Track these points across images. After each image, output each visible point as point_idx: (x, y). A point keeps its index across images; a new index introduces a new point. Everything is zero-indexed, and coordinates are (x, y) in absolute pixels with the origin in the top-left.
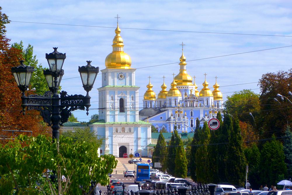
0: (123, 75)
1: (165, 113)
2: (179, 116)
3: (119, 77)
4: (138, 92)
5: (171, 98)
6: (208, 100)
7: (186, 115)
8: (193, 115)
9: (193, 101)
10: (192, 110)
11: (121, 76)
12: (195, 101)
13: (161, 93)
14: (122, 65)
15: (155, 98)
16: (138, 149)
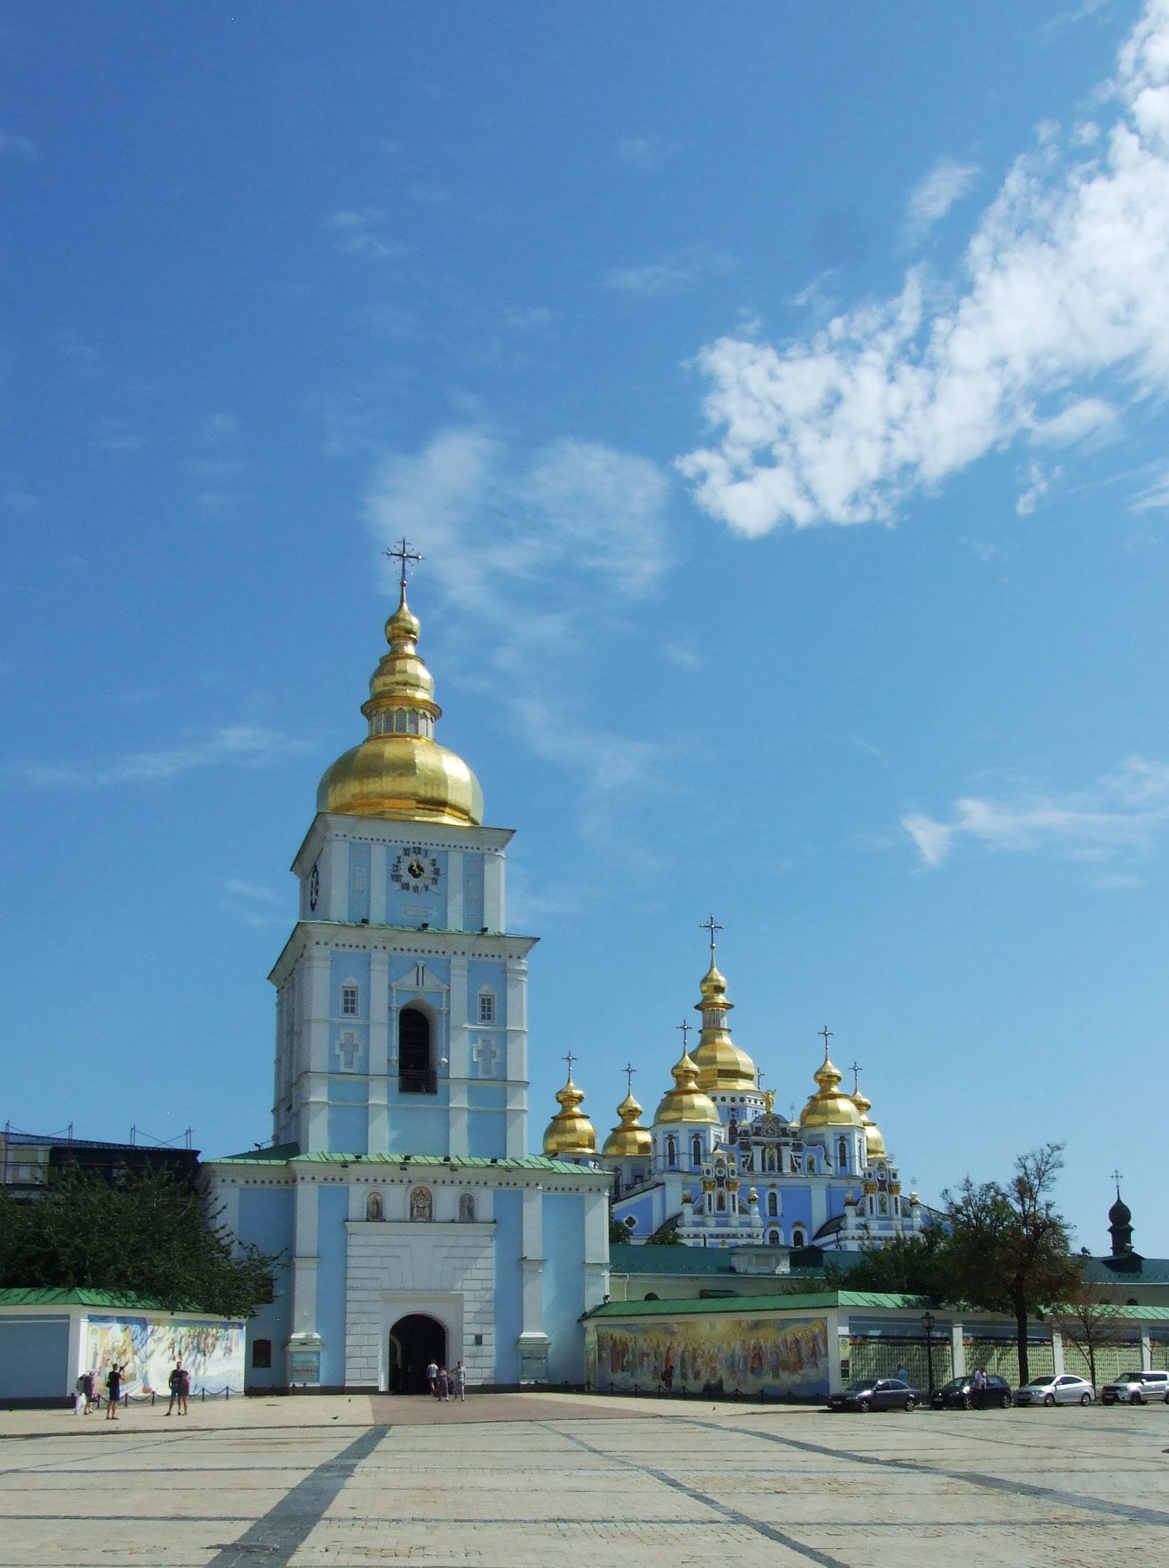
0: (425, 863)
1: (649, 1200)
2: (721, 1205)
3: (404, 871)
4: (524, 968)
5: (677, 1131)
6: (845, 1142)
7: (755, 1199)
8: (779, 1211)
9: (778, 1146)
10: (773, 1186)
11: (416, 872)
12: (786, 1144)
13: (617, 1136)
14: (421, 806)
15: (592, 1145)
16: (525, 1335)
